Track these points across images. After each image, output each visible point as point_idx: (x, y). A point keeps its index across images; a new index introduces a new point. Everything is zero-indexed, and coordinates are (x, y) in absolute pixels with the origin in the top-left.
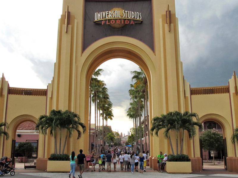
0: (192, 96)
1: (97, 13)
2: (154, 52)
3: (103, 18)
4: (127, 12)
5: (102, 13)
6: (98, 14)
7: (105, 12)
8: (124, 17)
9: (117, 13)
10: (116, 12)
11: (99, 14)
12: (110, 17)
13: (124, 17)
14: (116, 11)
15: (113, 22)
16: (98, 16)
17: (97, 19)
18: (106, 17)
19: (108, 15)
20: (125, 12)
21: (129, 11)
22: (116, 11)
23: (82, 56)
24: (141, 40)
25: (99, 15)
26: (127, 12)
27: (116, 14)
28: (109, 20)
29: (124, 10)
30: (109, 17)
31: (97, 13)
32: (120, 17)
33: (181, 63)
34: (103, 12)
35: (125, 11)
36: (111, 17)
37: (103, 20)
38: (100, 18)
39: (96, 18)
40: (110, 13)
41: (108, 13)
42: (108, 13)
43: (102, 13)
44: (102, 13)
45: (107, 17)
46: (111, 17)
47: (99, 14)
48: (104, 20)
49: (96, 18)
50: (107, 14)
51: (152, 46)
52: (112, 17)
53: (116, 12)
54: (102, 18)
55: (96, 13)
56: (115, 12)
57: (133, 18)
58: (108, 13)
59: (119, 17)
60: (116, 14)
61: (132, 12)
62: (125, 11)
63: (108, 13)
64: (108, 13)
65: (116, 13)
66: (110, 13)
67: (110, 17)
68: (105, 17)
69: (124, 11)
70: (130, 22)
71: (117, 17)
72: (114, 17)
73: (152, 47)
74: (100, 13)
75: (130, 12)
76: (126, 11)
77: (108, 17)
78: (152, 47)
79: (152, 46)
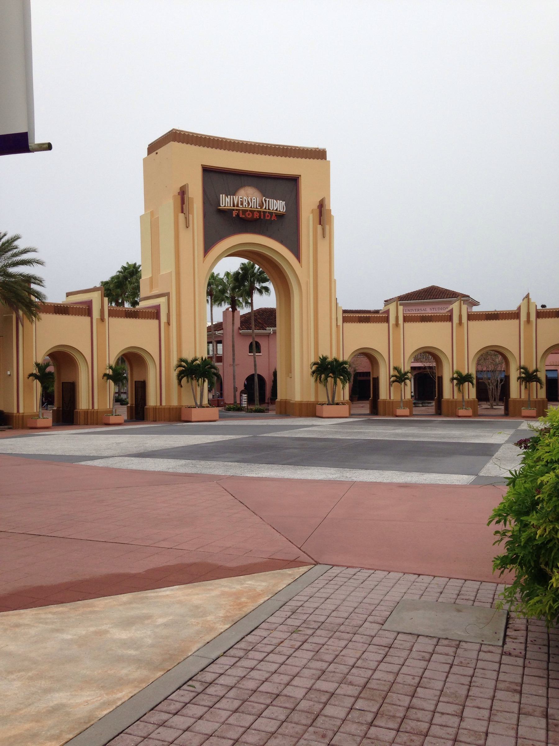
0: (345, 324)
3: (234, 206)
4: (269, 201)
7: (237, 197)
9: (255, 201)
10: (254, 199)
11: (228, 197)
12: (245, 205)
13: (264, 208)
14: (254, 198)
15: (249, 214)
16: (226, 202)
17: (225, 206)
18: (240, 206)
19: (241, 201)
20: (265, 201)
22: (254, 198)
24: (282, 242)
25: (228, 200)
26: (269, 201)
27: (254, 202)
28: (244, 211)
29: (264, 198)
30: (244, 206)
31: (224, 195)
32: (260, 208)
33: (335, 280)
34: (234, 196)
35: (266, 199)
36: (247, 206)
37: (234, 210)
38: (229, 206)
39: (223, 205)
40: (245, 200)
41: (241, 200)
42: (241, 198)
43: (232, 196)
45: (241, 205)
46: (247, 206)
47: (228, 197)
48: (237, 210)
49: (223, 205)
50: (240, 200)
51: (297, 253)
52: (248, 206)
53: (254, 199)
54: (232, 205)
55: (221, 195)
56: (253, 199)
59: (258, 207)
60: (254, 202)
61: (275, 200)
62: (266, 199)
63: (241, 200)
64: (241, 198)
65: (253, 201)
66: (245, 200)
67: (245, 205)
68: (238, 206)
69: (265, 199)
70: (271, 217)
71: (255, 207)
72: (251, 207)
73: (297, 254)
74: (229, 196)
76: (267, 199)
77: (242, 206)
79: (297, 253)
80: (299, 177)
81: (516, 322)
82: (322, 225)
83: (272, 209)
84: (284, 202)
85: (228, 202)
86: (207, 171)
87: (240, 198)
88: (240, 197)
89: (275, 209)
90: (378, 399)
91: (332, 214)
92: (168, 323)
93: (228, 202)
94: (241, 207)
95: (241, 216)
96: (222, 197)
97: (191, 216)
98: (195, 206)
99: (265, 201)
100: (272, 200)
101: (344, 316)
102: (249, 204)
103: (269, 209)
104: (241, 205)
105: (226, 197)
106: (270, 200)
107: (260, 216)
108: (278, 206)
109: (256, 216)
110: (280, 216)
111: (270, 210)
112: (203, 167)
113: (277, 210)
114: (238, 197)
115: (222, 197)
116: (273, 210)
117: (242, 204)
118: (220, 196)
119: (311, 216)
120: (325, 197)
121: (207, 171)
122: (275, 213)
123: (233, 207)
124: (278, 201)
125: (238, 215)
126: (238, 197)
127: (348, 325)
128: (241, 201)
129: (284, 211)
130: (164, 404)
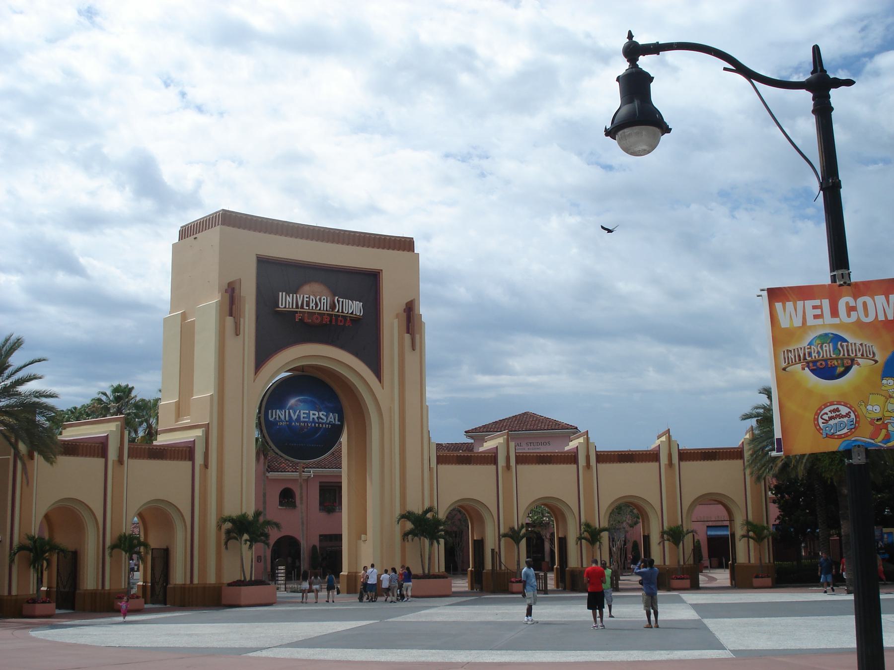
0: (440, 466)
1: (284, 293)
2: (380, 382)
4: (342, 302)
5: (296, 296)
6: (288, 296)
7: (302, 296)
8: (336, 311)
9: (325, 301)
10: (324, 299)
11: (289, 296)
12: (312, 307)
16: (286, 301)
17: (285, 307)
18: (305, 307)
19: (306, 301)
20: (338, 301)
21: (346, 299)
23: (256, 381)
25: (289, 299)
26: (342, 302)
27: (324, 302)
28: (311, 314)
30: (311, 308)
31: (284, 293)
33: (428, 406)
34: (298, 296)
35: (340, 299)
36: (314, 308)
37: (296, 312)
38: (291, 307)
39: (282, 305)
41: (308, 299)
42: (307, 298)
43: (295, 295)
44: (296, 296)
45: (306, 306)
46: (314, 308)
47: (289, 296)
49: (282, 305)
50: (305, 299)
51: (377, 371)
52: (316, 307)
53: (324, 299)
55: (281, 293)
57: (350, 314)
58: (309, 298)
60: (324, 302)
61: (350, 301)
62: (340, 299)
63: (308, 299)
64: (307, 298)
65: (323, 301)
67: (312, 307)
68: (302, 307)
71: (325, 309)
72: (320, 310)
73: (377, 372)
74: (291, 295)
75: (347, 300)
76: (341, 300)
77: (308, 308)
78: (377, 372)
79: (377, 371)
80: (379, 272)
81: (655, 465)
82: (411, 334)
83: (347, 312)
84: (361, 303)
85: (289, 303)
86: (263, 263)
87: (305, 297)
88: (305, 296)
89: (350, 312)
90: (483, 569)
91: (422, 320)
92: (206, 465)
93: (289, 303)
94: (307, 309)
95: (306, 320)
96: (282, 295)
97: (242, 320)
98: (247, 307)
99: (338, 301)
100: (347, 300)
101: (438, 454)
102: (316, 305)
103: (342, 312)
104: (306, 306)
105: (288, 296)
106: (345, 300)
107: (331, 321)
108: (355, 307)
109: (326, 320)
110: (355, 320)
111: (344, 313)
112: (257, 257)
113: (352, 313)
114: (303, 296)
115: (282, 295)
116: (347, 313)
117: (308, 305)
118: (279, 294)
119: (396, 322)
120: (414, 299)
121: (263, 263)
122: (350, 317)
123: (296, 308)
124: (354, 302)
125: (301, 320)
126: (303, 296)
127: (443, 468)
128: (306, 301)
129: (361, 315)
130: (196, 581)
